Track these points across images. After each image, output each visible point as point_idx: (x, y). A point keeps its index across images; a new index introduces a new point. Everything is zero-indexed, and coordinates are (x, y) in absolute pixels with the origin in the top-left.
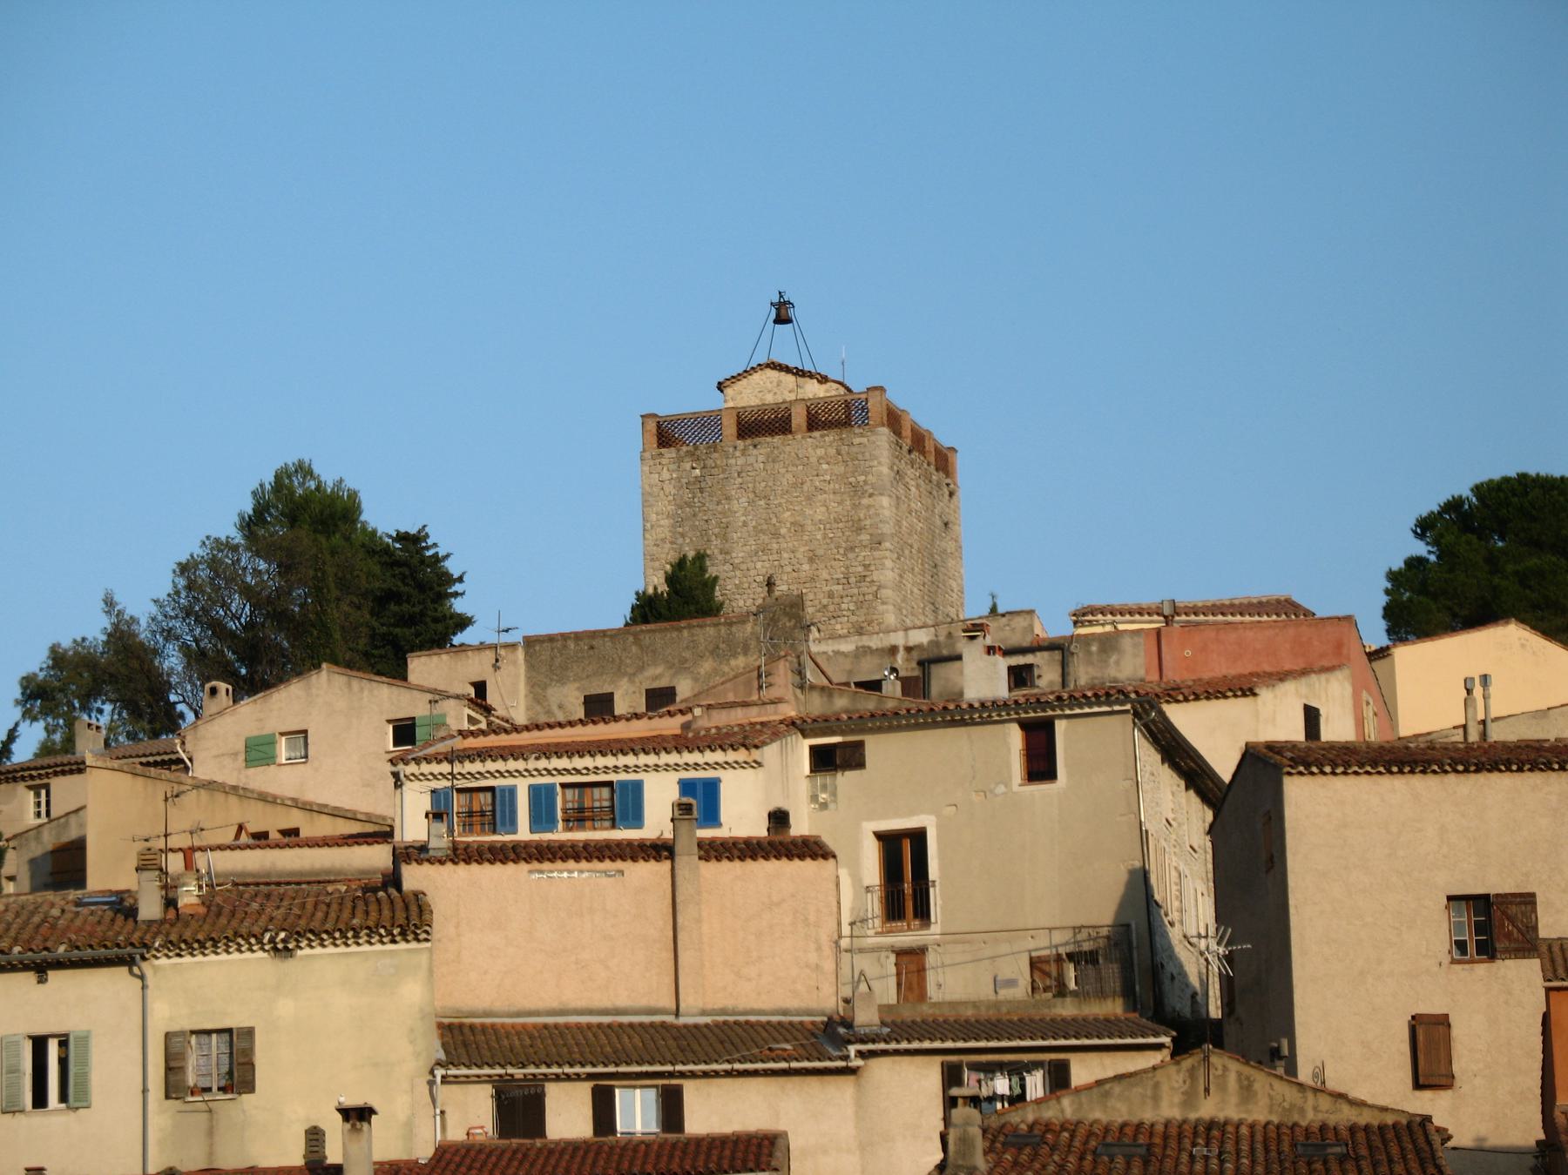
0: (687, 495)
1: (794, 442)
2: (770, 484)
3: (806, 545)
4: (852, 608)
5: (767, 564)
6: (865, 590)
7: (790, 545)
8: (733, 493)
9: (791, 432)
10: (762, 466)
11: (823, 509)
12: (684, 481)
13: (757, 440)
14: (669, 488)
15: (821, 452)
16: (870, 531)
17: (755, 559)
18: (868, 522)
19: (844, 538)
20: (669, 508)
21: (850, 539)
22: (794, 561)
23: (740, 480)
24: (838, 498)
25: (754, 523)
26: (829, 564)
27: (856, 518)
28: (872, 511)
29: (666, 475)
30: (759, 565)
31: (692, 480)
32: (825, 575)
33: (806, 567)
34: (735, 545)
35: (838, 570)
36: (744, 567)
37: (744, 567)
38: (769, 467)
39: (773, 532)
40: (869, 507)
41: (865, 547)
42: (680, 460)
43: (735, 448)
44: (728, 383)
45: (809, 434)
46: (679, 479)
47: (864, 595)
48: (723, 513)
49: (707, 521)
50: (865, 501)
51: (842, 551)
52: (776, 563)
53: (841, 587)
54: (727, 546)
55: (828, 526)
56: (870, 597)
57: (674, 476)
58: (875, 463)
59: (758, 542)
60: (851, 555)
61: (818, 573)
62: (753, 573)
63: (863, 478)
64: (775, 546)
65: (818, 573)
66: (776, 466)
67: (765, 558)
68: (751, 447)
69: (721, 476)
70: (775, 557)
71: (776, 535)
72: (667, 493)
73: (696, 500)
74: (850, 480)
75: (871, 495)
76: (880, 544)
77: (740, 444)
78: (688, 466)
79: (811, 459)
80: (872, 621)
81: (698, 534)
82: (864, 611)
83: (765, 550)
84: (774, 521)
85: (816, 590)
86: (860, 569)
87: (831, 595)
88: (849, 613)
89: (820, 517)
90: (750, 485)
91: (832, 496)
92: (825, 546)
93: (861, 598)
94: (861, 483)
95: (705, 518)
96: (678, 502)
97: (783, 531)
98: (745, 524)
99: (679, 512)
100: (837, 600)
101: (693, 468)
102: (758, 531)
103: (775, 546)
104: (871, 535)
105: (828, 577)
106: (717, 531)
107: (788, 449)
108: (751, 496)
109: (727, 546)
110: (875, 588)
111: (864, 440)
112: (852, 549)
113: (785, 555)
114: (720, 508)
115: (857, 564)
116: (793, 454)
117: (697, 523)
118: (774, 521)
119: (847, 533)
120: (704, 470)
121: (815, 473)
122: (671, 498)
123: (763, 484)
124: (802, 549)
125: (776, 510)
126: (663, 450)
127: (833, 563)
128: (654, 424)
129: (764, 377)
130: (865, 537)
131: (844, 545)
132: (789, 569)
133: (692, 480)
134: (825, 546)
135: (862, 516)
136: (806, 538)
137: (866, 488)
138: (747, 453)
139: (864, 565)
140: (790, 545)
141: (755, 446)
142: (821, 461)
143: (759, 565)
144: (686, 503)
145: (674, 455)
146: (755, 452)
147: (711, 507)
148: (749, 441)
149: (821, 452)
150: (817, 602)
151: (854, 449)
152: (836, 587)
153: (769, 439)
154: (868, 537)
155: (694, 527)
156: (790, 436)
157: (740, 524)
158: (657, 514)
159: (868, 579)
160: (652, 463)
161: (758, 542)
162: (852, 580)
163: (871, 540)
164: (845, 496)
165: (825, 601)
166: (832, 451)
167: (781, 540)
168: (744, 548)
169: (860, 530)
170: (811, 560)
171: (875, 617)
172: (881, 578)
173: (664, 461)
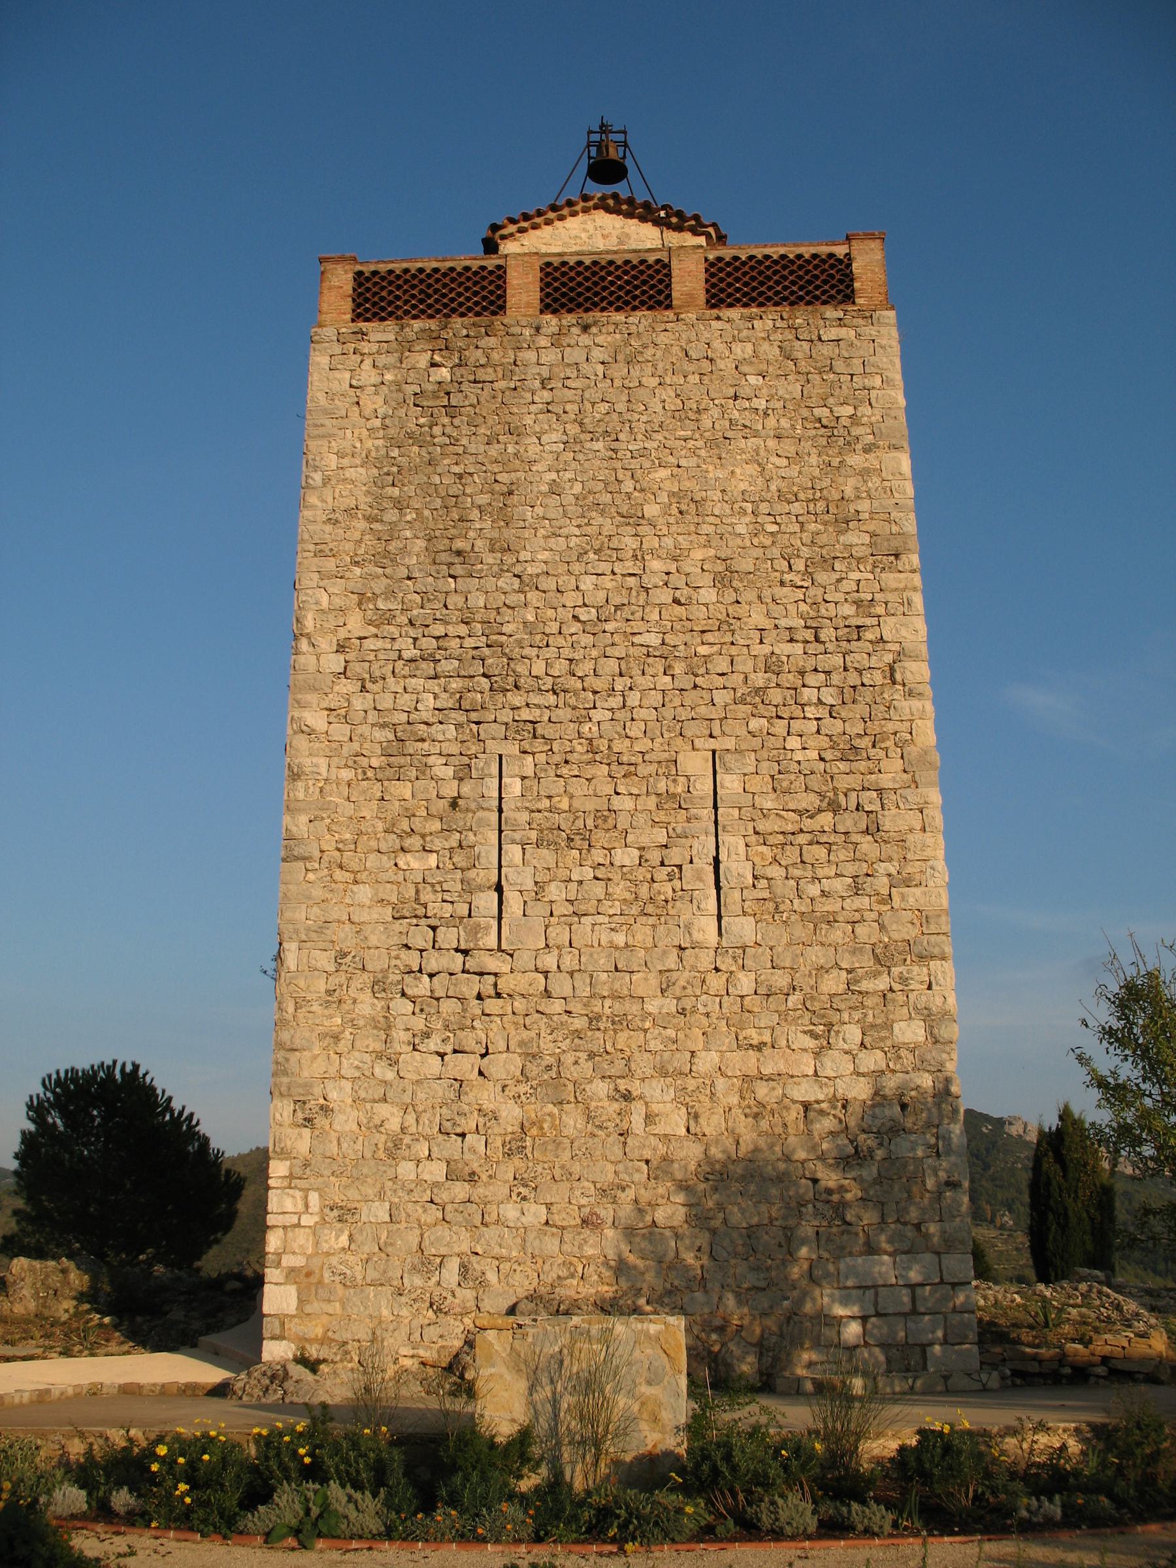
0: (415, 419)
1: (680, 326)
2: (621, 407)
3: (708, 545)
4: (830, 701)
5: (607, 582)
6: (858, 659)
7: (668, 542)
8: (528, 420)
9: (669, 307)
10: (600, 369)
11: (752, 469)
12: (411, 389)
13: (589, 317)
14: (373, 402)
15: (743, 350)
16: (871, 528)
17: (577, 568)
18: (864, 506)
19: (806, 537)
20: (369, 444)
21: (823, 539)
22: (677, 580)
23: (547, 395)
24: (789, 447)
25: (577, 488)
26: (767, 593)
27: (836, 496)
28: (874, 482)
29: (368, 375)
30: (587, 583)
31: (430, 387)
32: (758, 617)
33: (708, 595)
34: (527, 534)
35: (792, 608)
36: (549, 584)
37: (549, 584)
38: (619, 371)
39: (624, 509)
40: (865, 473)
41: (859, 560)
42: (406, 346)
43: (538, 329)
44: (512, 228)
45: (715, 312)
46: (398, 386)
47: (860, 672)
48: (502, 462)
49: (460, 476)
50: (856, 460)
51: (799, 565)
52: (632, 581)
53: (798, 648)
54: (508, 533)
55: (764, 508)
56: (878, 677)
57: (389, 377)
58: (877, 381)
59: (588, 530)
60: (822, 577)
61: (741, 610)
62: (571, 599)
63: (849, 410)
64: (631, 543)
65: (741, 610)
66: (636, 372)
67: (605, 567)
68: (575, 330)
69: (502, 384)
70: (630, 566)
71: (633, 518)
72: (368, 412)
73: (437, 430)
74: (817, 412)
75: (867, 450)
76: (897, 556)
77: (551, 322)
78: (423, 360)
79: (721, 364)
80: (884, 736)
81: (438, 503)
82: (861, 709)
83: (606, 549)
84: (628, 486)
85: (734, 650)
86: (848, 610)
87: (772, 665)
88: (823, 712)
89: (743, 486)
90: (568, 407)
91: (772, 443)
92: (758, 552)
93: (853, 679)
94: (844, 421)
95: (457, 469)
96: (392, 432)
97: (651, 510)
98: (555, 490)
99: (395, 453)
100: (789, 679)
101: (433, 365)
102: (587, 504)
103: (631, 543)
104: (873, 535)
105: (767, 624)
106: (483, 499)
107: (662, 339)
108: (573, 429)
109: (508, 533)
110: (889, 658)
111: (843, 332)
112: (828, 563)
113: (656, 565)
114: (494, 451)
115: (840, 597)
116: (676, 350)
117: (437, 479)
118: (628, 486)
119: (812, 527)
120: (459, 372)
121: (731, 392)
122: (377, 423)
123: (603, 408)
124: (698, 554)
125: (634, 464)
126: (364, 325)
127: (779, 592)
128: (350, 276)
129: (590, 226)
130: (856, 539)
131: (805, 552)
132: (665, 596)
133: (430, 387)
134: (758, 552)
135: (849, 492)
136: (706, 529)
137: (856, 431)
138: (565, 341)
139: (858, 603)
140: (668, 542)
141: (585, 328)
142: (744, 368)
143: (587, 583)
144: (410, 435)
145: (392, 337)
146: (585, 340)
147: (472, 449)
148: (569, 319)
149: (743, 350)
150: (737, 679)
151: (826, 350)
152: (784, 649)
153: (619, 317)
154: (866, 539)
155: (428, 489)
156: (670, 314)
157: (545, 488)
158: (340, 455)
159: (869, 635)
160: (337, 349)
161: (588, 530)
162: (827, 634)
163: (871, 545)
164: (806, 445)
165: (759, 679)
166: (771, 351)
167: (644, 529)
168: (552, 542)
169: (844, 523)
170: (722, 581)
171: (890, 727)
172: (904, 632)
173: (365, 347)
